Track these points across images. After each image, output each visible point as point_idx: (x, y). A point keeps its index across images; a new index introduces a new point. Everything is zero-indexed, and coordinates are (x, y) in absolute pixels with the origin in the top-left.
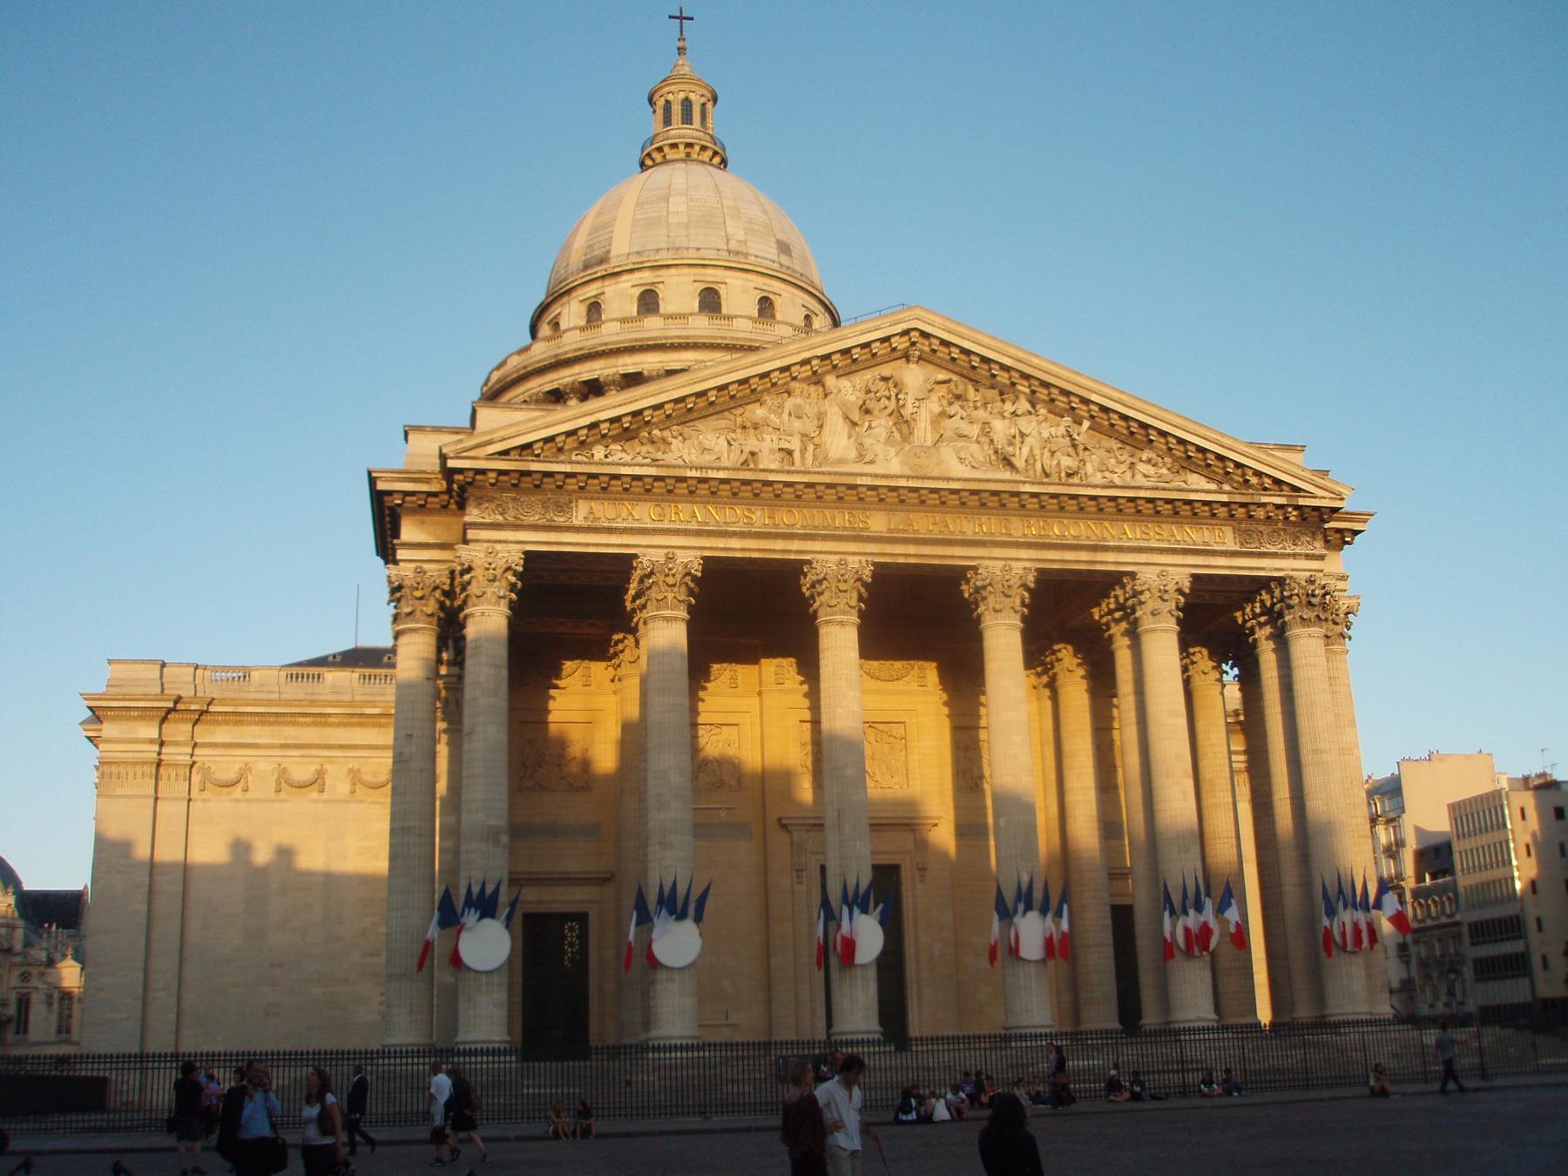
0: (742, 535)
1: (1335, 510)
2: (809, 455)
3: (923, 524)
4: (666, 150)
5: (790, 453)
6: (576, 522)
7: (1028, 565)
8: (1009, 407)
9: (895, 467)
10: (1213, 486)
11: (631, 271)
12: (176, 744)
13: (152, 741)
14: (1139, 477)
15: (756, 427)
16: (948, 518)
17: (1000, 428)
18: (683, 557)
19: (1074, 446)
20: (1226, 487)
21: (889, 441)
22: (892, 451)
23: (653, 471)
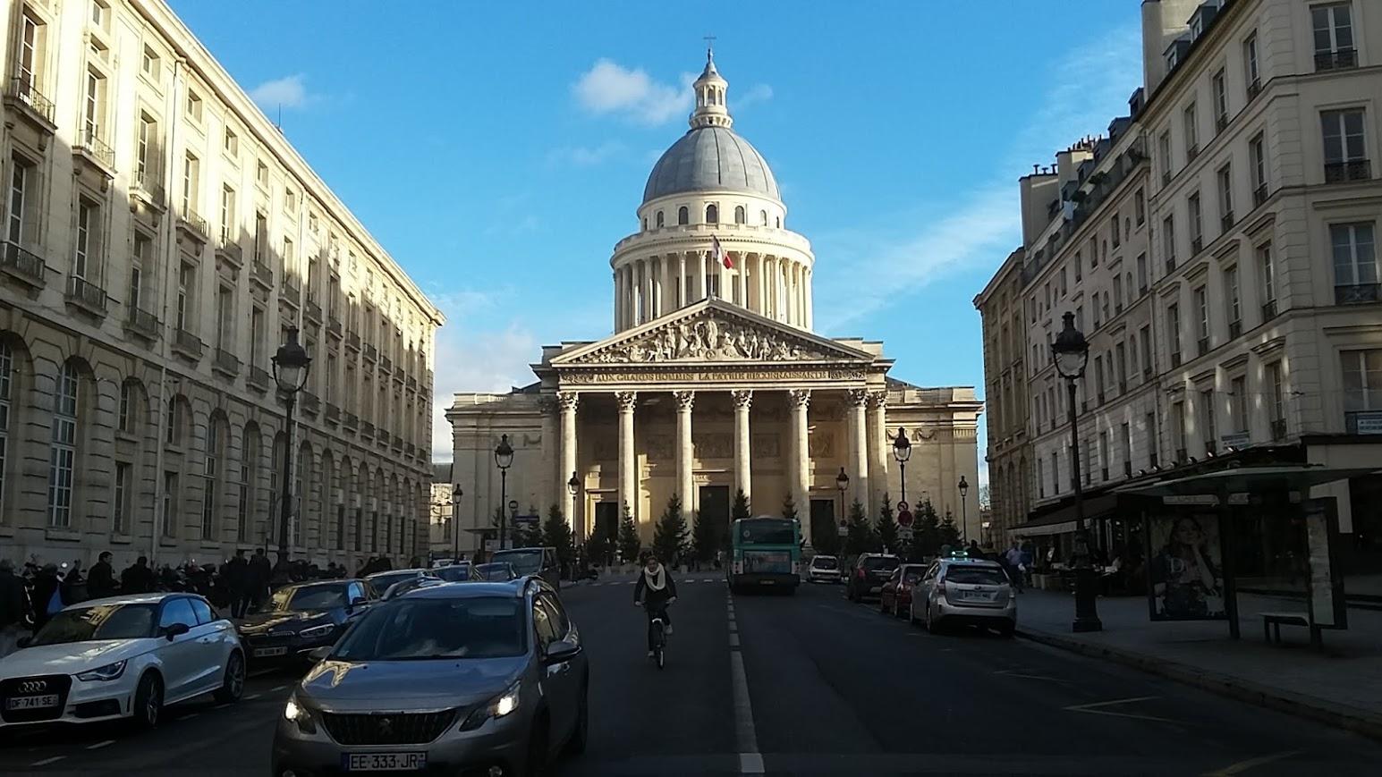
4: (700, 120)
6: (595, 382)
8: (746, 332)
12: (483, 427)
13: (474, 427)
17: (742, 339)
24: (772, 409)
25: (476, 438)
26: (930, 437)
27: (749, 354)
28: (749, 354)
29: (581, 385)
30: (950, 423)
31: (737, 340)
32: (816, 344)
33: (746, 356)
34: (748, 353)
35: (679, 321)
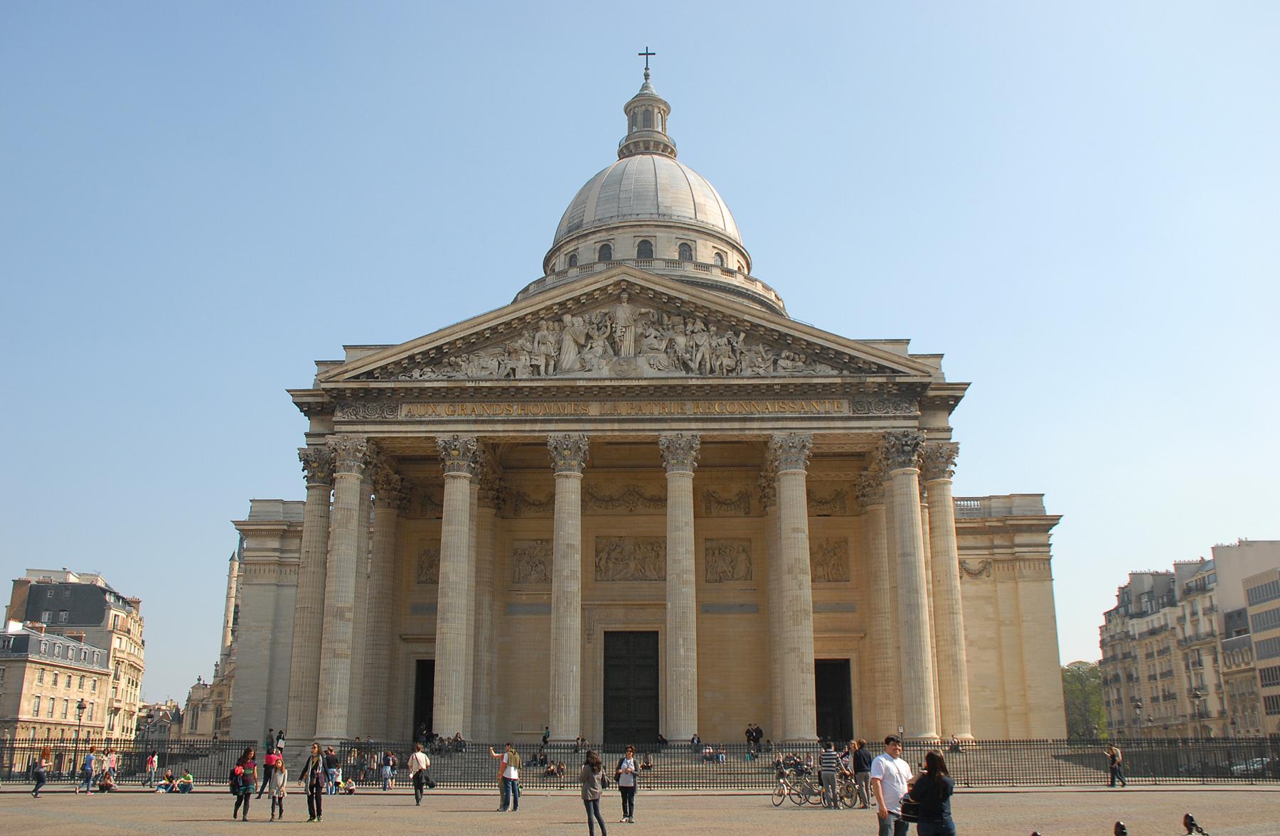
0: (504, 422)
1: (925, 386)
2: (551, 368)
3: (624, 409)
4: (632, 147)
5: (538, 367)
6: (400, 418)
7: (694, 433)
8: (690, 327)
9: (605, 372)
10: (835, 372)
11: (594, 233)
12: (290, 551)
13: (274, 550)
14: (779, 369)
15: (516, 351)
16: (643, 404)
17: (681, 341)
18: (465, 437)
19: (733, 351)
20: (845, 372)
21: (601, 357)
22: (604, 362)
23: (445, 384)
24: (738, 477)
25: (277, 568)
26: (980, 573)
27: (694, 365)
28: (694, 365)
29: (375, 423)
30: (1009, 551)
31: (671, 342)
32: (822, 348)
33: (687, 368)
34: (692, 365)
35: (562, 305)
